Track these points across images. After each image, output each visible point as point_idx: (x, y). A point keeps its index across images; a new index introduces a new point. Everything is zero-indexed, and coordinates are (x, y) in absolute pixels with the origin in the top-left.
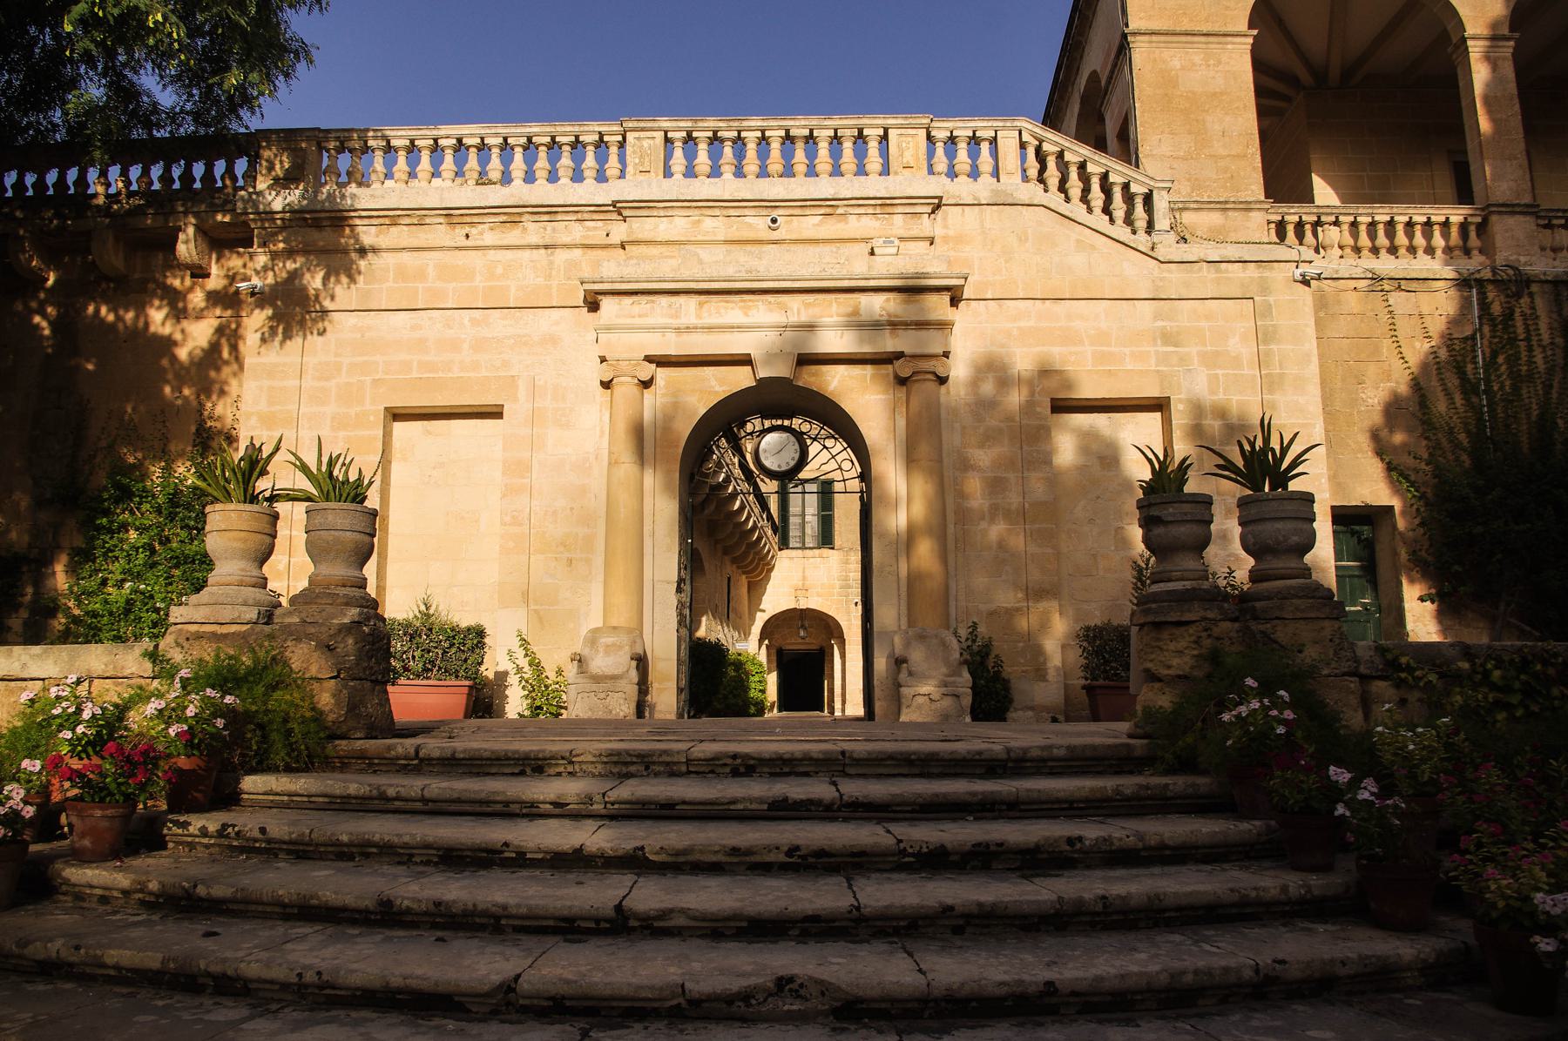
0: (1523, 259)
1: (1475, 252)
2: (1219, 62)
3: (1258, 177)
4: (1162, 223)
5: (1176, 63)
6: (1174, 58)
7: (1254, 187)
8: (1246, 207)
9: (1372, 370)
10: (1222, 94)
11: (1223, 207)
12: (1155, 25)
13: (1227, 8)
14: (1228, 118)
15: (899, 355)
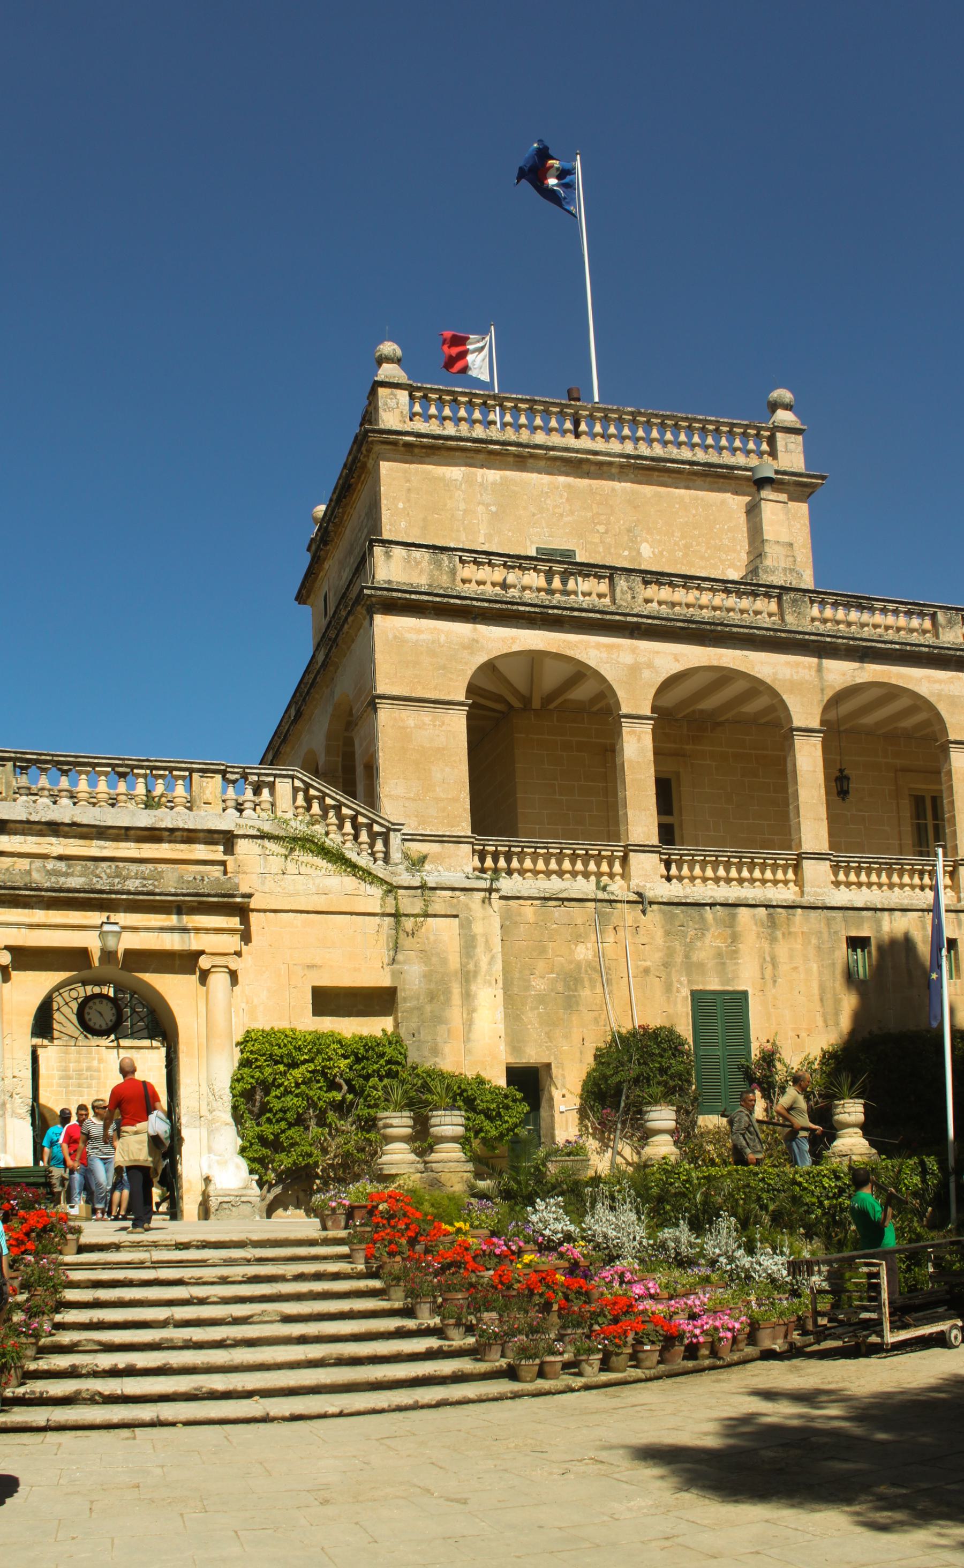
0: (648, 885)
1: (618, 878)
2: (443, 724)
3: (467, 816)
4: (396, 856)
5: (411, 723)
6: (410, 717)
7: (465, 828)
8: (457, 840)
9: (541, 965)
10: (443, 749)
11: (440, 839)
12: (396, 692)
13: (451, 679)
14: (447, 769)
15: (202, 952)
